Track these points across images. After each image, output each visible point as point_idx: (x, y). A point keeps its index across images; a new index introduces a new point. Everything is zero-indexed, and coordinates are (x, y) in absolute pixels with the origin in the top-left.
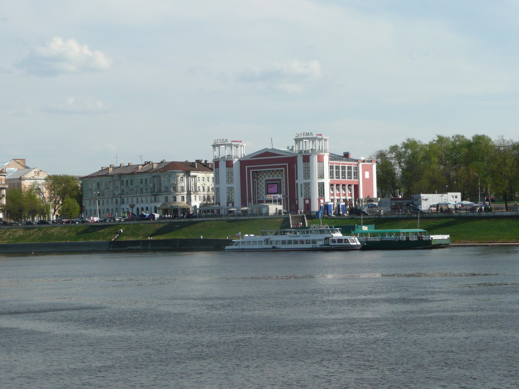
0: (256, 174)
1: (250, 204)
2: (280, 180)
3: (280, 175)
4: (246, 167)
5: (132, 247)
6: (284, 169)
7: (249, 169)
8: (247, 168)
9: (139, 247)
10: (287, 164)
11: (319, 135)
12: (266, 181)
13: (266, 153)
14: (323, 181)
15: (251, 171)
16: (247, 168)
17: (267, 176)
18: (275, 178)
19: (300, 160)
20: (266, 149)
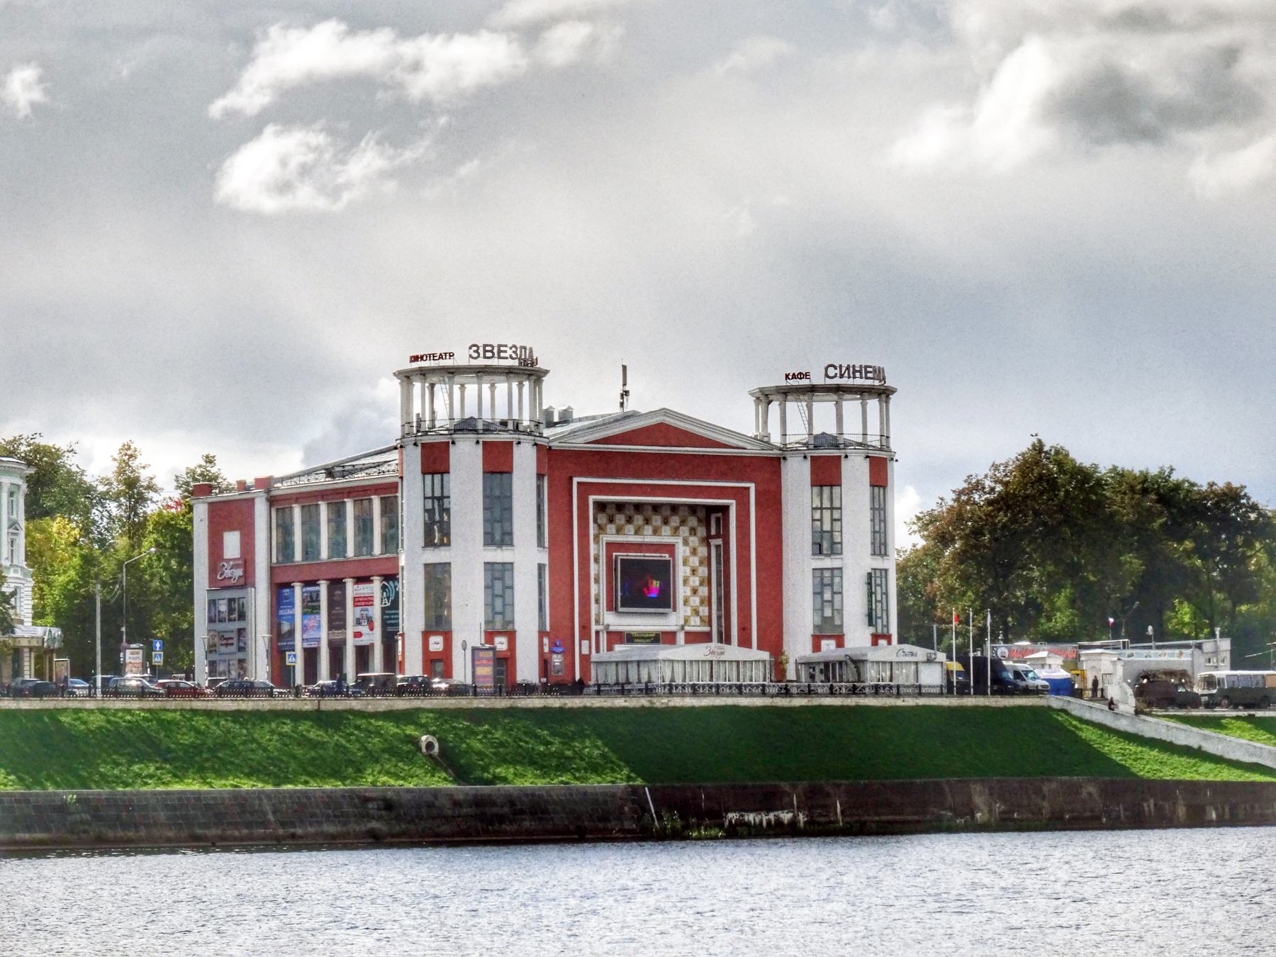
0: (712, 518)
1: (585, 643)
2: (670, 548)
3: (666, 530)
4: (576, 480)
5: (751, 817)
6: (732, 503)
7: (585, 489)
8: (579, 483)
9: (786, 816)
10: (752, 486)
11: (794, 376)
12: (611, 546)
13: (662, 431)
14: (885, 567)
15: (592, 498)
16: (579, 483)
17: (611, 528)
18: (648, 538)
19: (796, 475)
20: (665, 412)
